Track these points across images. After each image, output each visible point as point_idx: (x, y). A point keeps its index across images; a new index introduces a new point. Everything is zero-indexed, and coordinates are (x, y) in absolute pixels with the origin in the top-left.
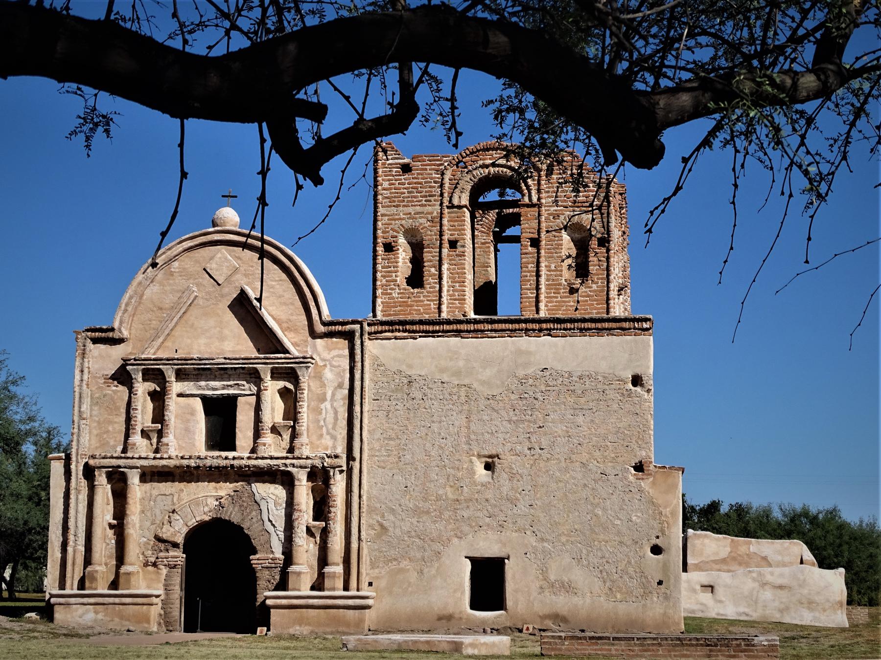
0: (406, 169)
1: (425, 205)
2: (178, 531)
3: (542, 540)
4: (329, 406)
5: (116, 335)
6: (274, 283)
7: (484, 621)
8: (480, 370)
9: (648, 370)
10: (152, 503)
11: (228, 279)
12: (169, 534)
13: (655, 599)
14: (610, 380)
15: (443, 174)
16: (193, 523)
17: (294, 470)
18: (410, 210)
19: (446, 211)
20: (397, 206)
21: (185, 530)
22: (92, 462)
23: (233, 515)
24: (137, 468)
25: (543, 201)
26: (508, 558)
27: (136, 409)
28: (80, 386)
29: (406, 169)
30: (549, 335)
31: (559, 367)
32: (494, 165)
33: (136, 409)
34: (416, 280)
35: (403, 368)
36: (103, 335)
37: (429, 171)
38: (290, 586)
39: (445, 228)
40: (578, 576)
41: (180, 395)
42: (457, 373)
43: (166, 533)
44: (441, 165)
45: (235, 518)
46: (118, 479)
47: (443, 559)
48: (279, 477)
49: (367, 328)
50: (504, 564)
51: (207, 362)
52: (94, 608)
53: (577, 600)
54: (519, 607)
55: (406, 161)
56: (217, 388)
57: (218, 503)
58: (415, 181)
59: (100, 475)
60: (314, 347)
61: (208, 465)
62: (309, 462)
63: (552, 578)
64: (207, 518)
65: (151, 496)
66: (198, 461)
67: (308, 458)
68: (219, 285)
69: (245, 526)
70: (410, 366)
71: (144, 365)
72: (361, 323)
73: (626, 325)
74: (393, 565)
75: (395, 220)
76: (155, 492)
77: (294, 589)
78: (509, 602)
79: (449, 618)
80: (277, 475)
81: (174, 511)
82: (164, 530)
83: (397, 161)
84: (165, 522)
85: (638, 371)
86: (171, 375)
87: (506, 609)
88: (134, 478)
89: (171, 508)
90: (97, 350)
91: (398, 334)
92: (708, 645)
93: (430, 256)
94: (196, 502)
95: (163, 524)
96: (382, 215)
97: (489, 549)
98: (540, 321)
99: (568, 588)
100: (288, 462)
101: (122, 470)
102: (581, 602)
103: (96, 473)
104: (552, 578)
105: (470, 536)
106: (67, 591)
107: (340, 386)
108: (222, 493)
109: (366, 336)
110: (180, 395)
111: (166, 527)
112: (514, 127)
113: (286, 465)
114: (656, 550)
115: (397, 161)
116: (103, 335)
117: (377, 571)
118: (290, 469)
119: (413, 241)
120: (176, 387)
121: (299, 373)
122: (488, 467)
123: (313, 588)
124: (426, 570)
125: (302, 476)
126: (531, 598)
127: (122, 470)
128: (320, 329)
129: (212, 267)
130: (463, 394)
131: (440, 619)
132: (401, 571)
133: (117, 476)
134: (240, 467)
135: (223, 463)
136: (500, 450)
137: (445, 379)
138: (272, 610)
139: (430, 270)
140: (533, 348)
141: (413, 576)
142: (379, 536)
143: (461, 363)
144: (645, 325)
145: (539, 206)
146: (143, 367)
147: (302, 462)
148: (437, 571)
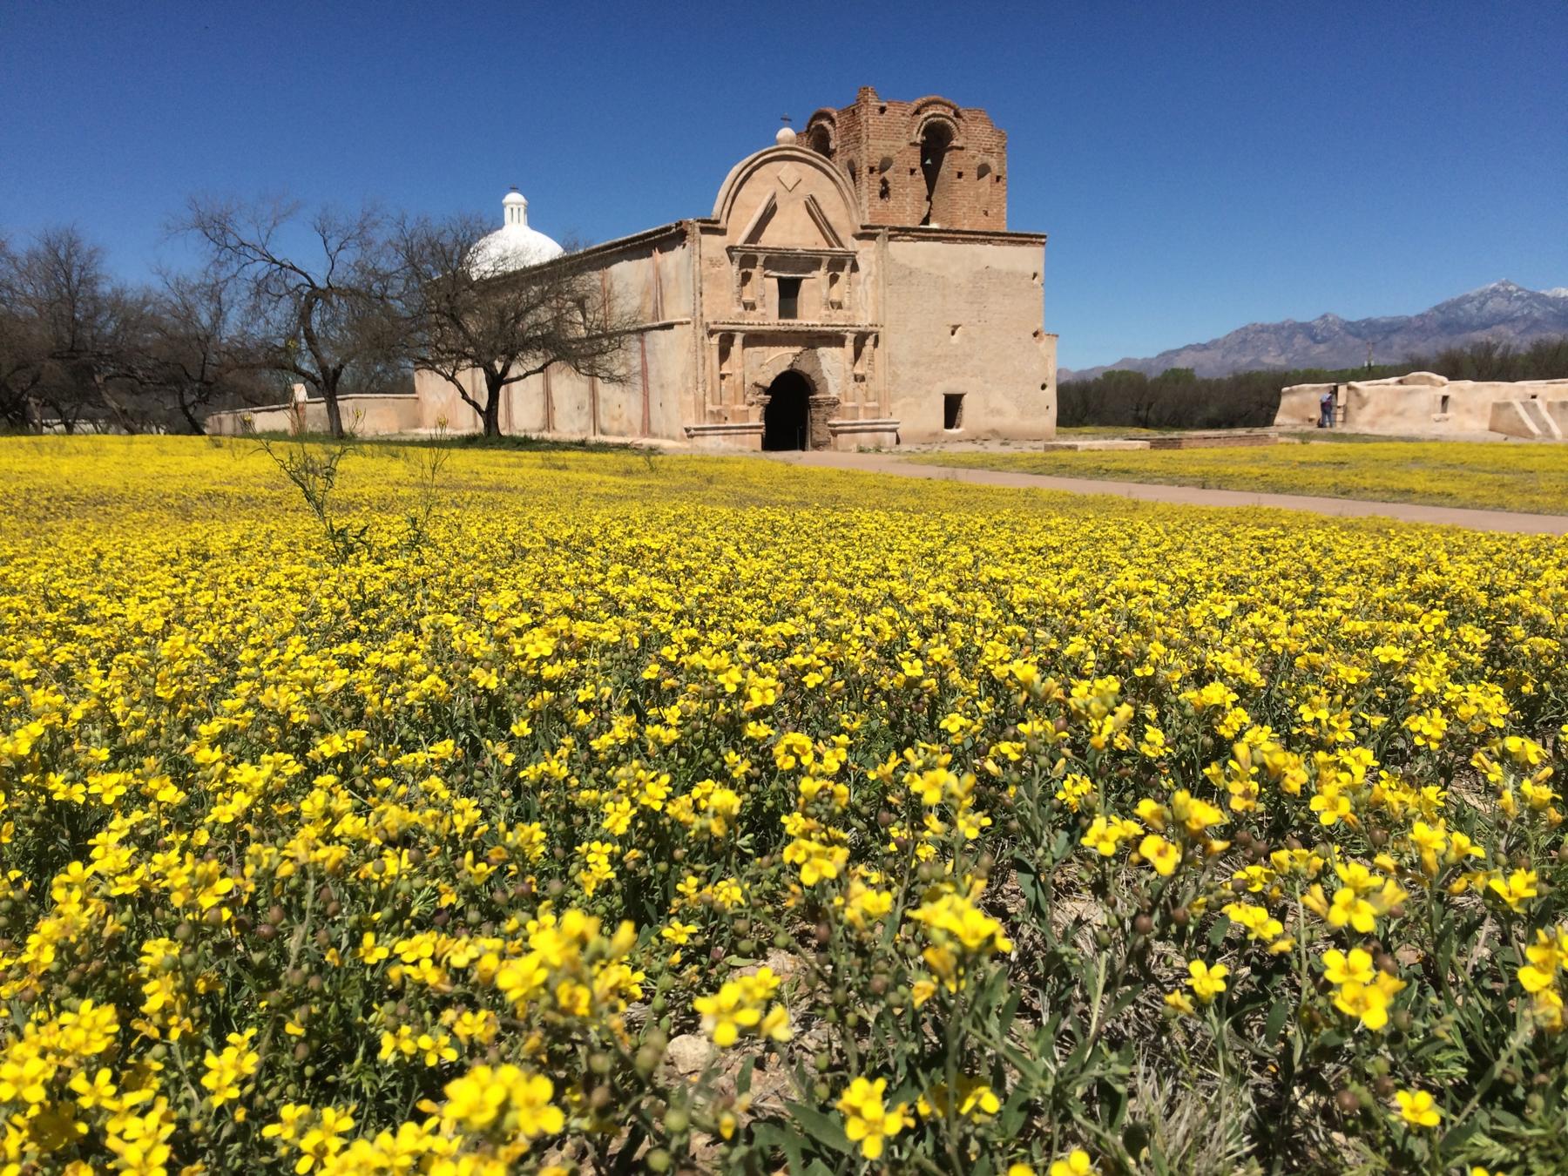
2: (767, 379)
5: (720, 226)
9: (1041, 272)
14: (1023, 276)
16: (778, 372)
23: (805, 367)
31: (995, 266)
63: (992, 405)
79: (935, 434)
88: (738, 341)
90: (717, 239)
94: (781, 357)
97: (955, 389)
99: (999, 412)
107: (869, 274)
114: (1044, 387)
125: (850, 337)
136: (963, 322)
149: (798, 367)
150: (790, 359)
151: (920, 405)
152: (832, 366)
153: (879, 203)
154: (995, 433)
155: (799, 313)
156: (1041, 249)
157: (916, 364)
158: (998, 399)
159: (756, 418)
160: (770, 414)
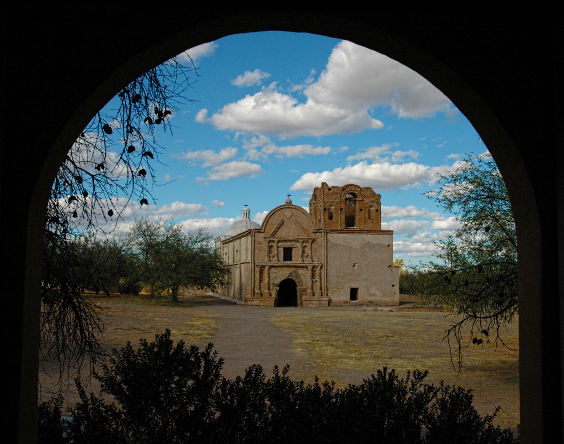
0: (330, 189)
2: (278, 281)
3: (368, 283)
7: (355, 303)
14: (384, 246)
16: (282, 280)
21: (280, 281)
31: (372, 242)
35: (334, 241)
40: (377, 292)
42: (348, 243)
45: (294, 278)
46: (262, 268)
53: (375, 298)
63: (371, 292)
74: (332, 290)
76: (272, 272)
79: (346, 302)
94: (284, 274)
97: (354, 286)
99: (374, 295)
108: (290, 272)
112: (481, 217)
114: (393, 286)
129: (286, 214)
132: (336, 291)
135: (292, 265)
147: (311, 265)
149: (290, 277)
151: (340, 292)
152: (305, 276)
153: (328, 221)
154: (371, 302)
155: (293, 259)
157: (338, 277)
158: (373, 290)
159: (274, 294)
160: (279, 293)
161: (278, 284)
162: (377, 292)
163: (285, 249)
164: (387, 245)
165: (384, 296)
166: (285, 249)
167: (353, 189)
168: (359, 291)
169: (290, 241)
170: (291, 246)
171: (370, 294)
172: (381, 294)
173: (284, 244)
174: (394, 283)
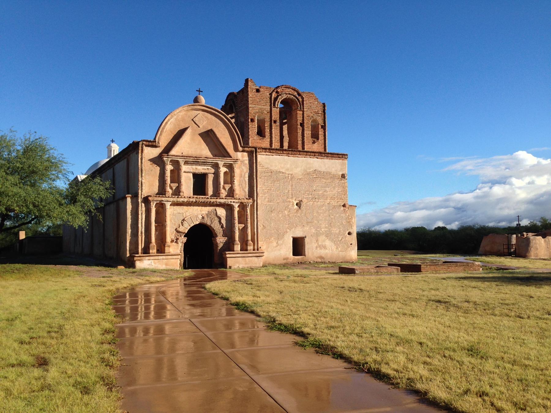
1: (265, 106)
2: (185, 228)
4: (243, 179)
6: (221, 129)
7: (298, 259)
8: (295, 169)
10: (174, 216)
11: (203, 126)
12: (182, 230)
13: (350, 250)
15: (271, 94)
16: (192, 225)
17: (234, 204)
18: (260, 106)
19: (273, 109)
20: (255, 104)
21: (189, 228)
22: (150, 198)
24: (170, 201)
25: (305, 110)
26: (305, 237)
27: (168, 177)
28: (141, 165)
29: (258, 91)
30: (317, 158)
31: (320, 170)
32: (289, 94)
33: (168, 177)
34: (261, 133)
35: (269, 166)
36: (150, 143)
37: (266, 93)
38: (235, 250)
39: (273, 115)
41: (185, 172)
42: (288, 170)
43: (181, 229)
44: (271, 91)
45: (209, 223)
47: (285, 238)
48: (226, 206)
49: (258, 150)
50: (305, 239)
51: (199, 159)
52: (154, 262)
54: (310, 254)
55: (258, 88)
56: (200, 169)
57: (202, 217)
58: (261, 96)
59: (153, 204)
60: (237, 156)
61: (201, 201)
62: (240, 201)
63: (320, 244)
64: (198, 223)
65: (174, 213)
66: (196, 199)
67: (239, 199)
68: (199, 127)
69: (212, 226)
70: (272, 166)
71: (171, 158)
72: (256, 148)
73: (341, 156)
75: (254, 109)
76: (175, 212)
77: (237, 251)
78: (306, 253)
79: (287, 259)
80: (225, 206)
81: (183, 220)
82: (180, 228)
83: (255, 87)
84: (180, 225)
85: (344, 173)
86: (182, 163)
87: (305, 255)
88: (168, 205)
89: (182, 218)
91: (267, 153)
92: (464, 266)
93: (267, 125)
95: (179, 225)
96: (250, 107)
97: (299, 234)
98: (304, 152)
99: (325, 247)
100: (232, 200)
101: (163, 202)
102: (328, 252)
103: (152, 203)
104: (320, 244)
105: (294, 229)
106: (140, 255)
109: (258, 153)
110: (185, 172)
111: (181, 226)
113: (231, 202)
114: (349, 234)
115: (255, 87)
116: (150, 143)
117: (262, 242)
118: (232, 203)
119: (259, 119)
120: (184, 168)
121: (234, 166)
122: (297, 204)
123: (241, 251)
124: (279, 242)
125: (236, 205)
126: (313, 251)
127: (163, 202)
128: (240, 149)
130: (290, 177)
131: (284, 259)
133: (158, 205)
134: (214, 202)
135: (206, 200)
137: (283, 171)
138: (228, 259)
139: (267, 130)
140: (312, 162)
141: (275, 244)
142: (263, 229)
143: (288, 166)
144: (346, 157)
145: (303, 111)
146: (172, 159)
147: (237, 201)
148: (283, 242)
150: (200, 217)
153: (256, 137)
156: (346, 161)
160: (187, 247)
161: (186, 232)
162: (328, 243)
163: (195, 175)
164: (341, 173)
165: (337, 248)
166: (195, 175)
167: (290, 93)
168: (306, 240)
169: (204, 163)
170: (203, 171)
171: (320, 246)
172: (334, 247)
173: (194, 167)
174: (351, 231)
